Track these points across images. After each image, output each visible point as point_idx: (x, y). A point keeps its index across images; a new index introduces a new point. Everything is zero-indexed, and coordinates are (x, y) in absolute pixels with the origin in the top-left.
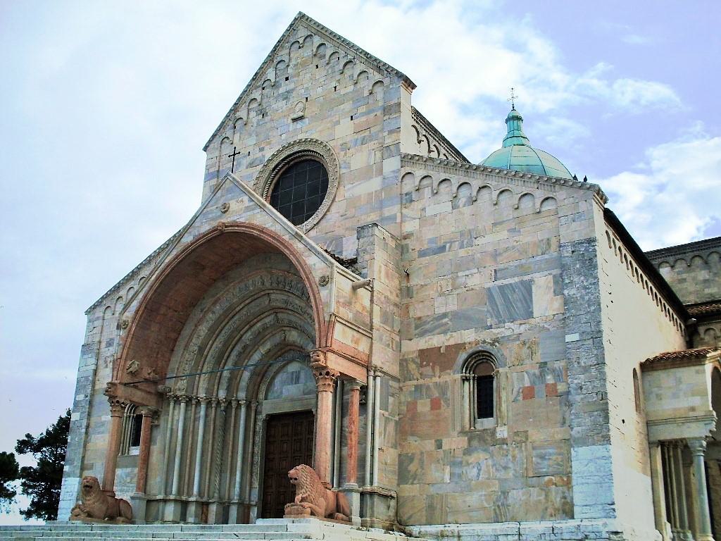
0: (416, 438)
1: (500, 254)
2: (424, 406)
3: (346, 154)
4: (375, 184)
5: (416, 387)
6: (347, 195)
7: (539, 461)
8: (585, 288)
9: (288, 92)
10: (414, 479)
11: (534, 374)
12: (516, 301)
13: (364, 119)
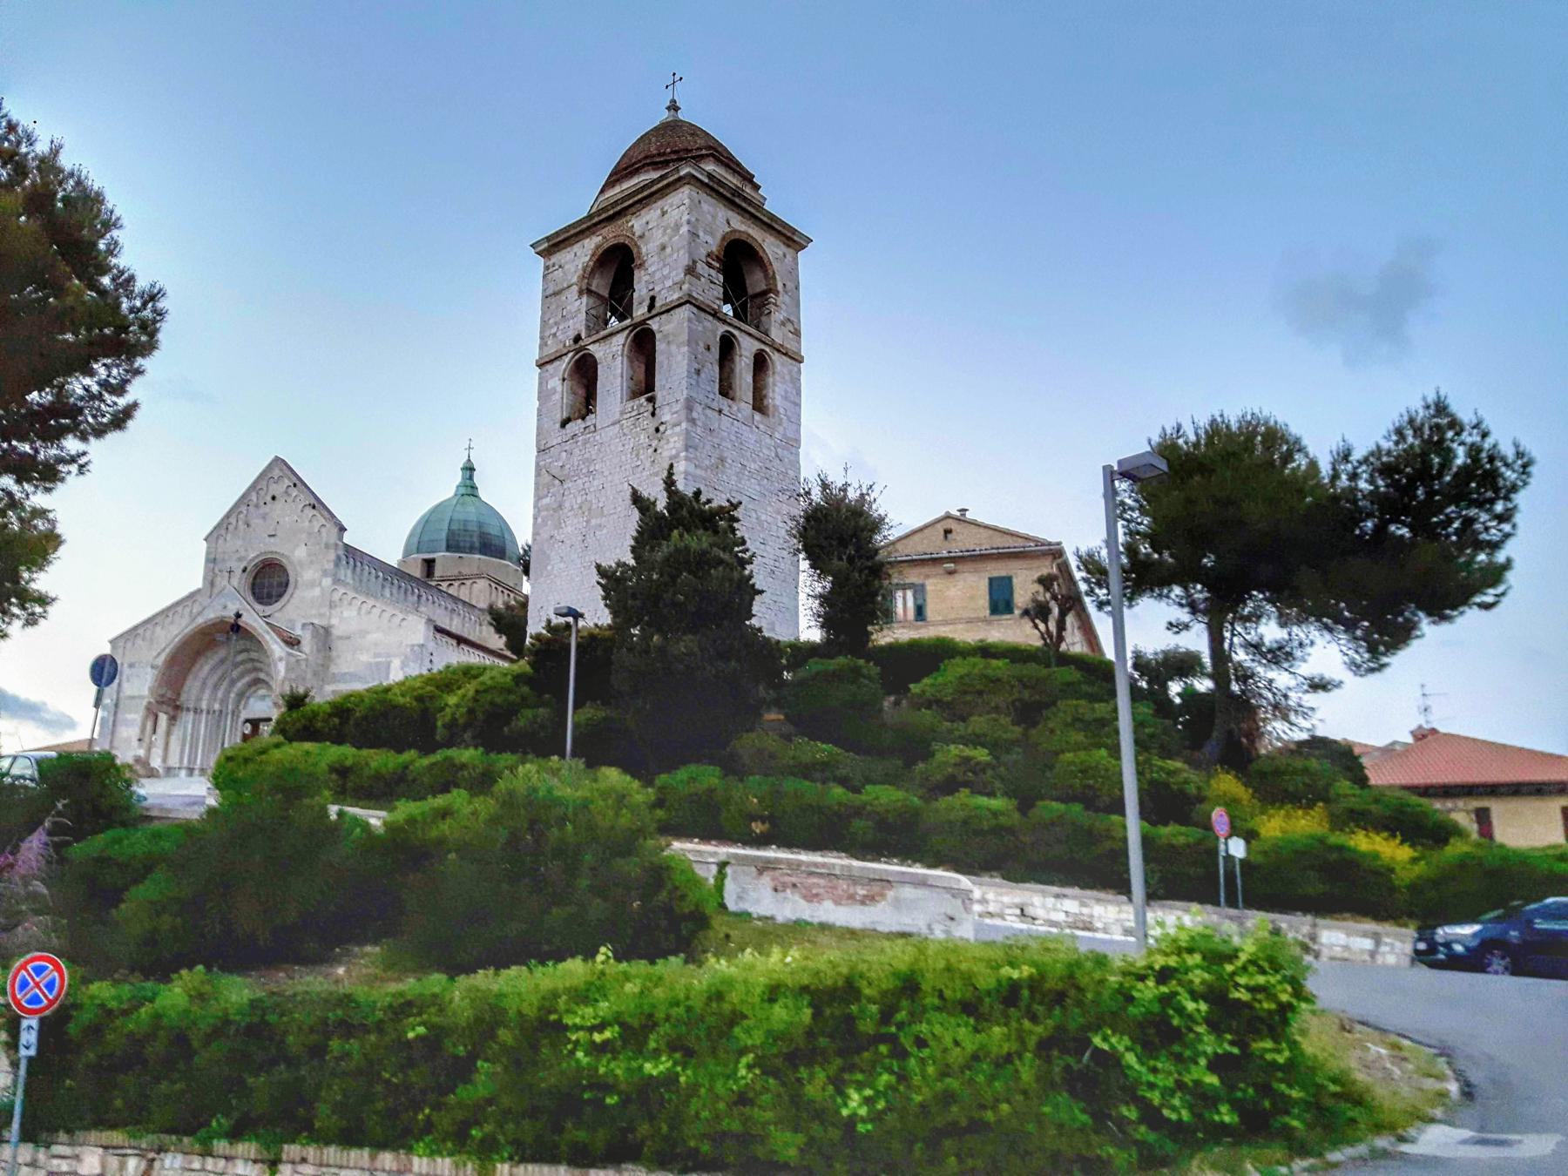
4: (317, 591)
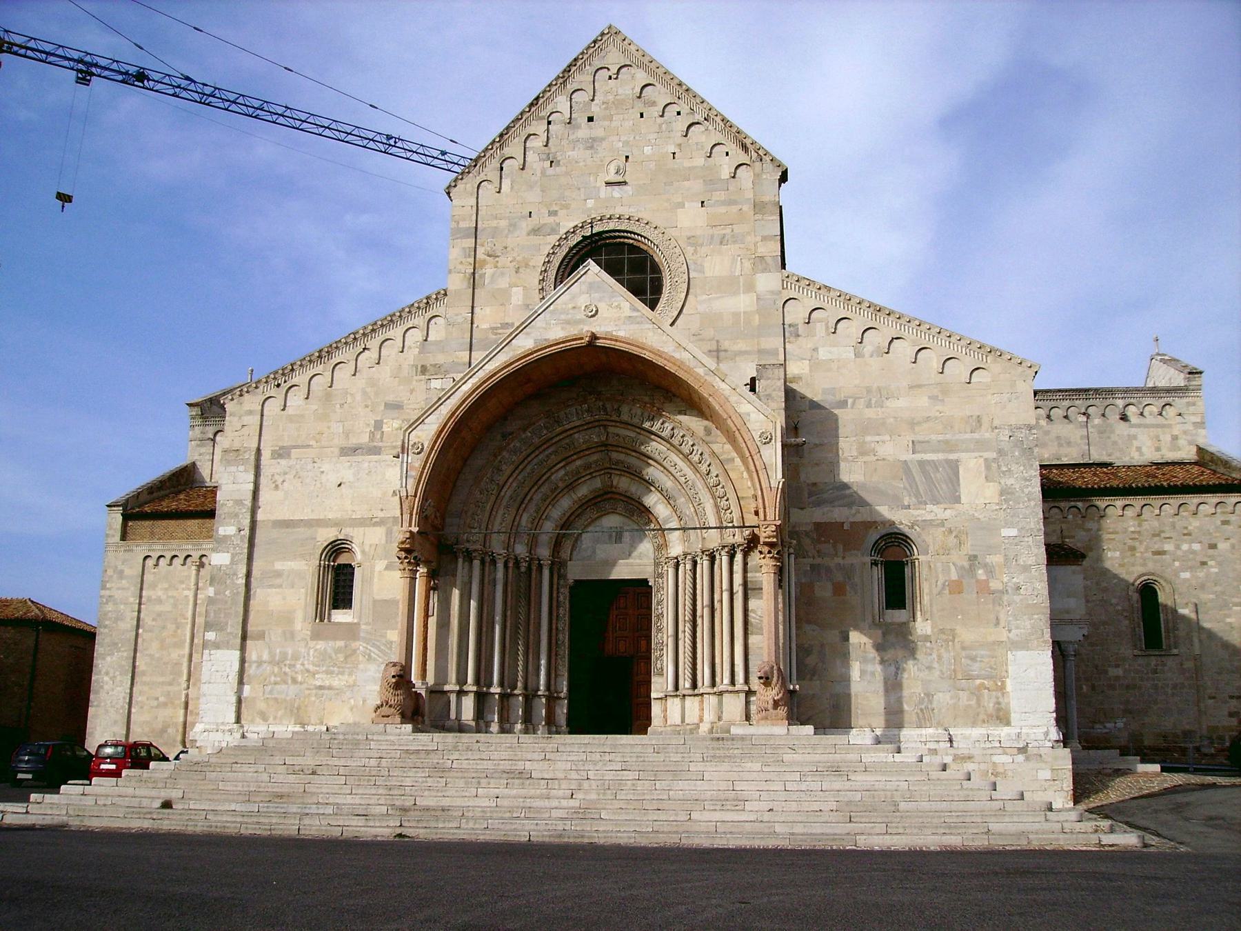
0: (815, 627)
1: (919, 423)
2: (824, 591)
3: (695, 251)
4: (743, 302)
5: (812, 566)
6: (701, 308)
7: (969, 662)
8: (1026, 480)
9: (594, 140)
10: (813, 675)
11: (962, 567)
12: (942, 481)
13: (723, 210)
